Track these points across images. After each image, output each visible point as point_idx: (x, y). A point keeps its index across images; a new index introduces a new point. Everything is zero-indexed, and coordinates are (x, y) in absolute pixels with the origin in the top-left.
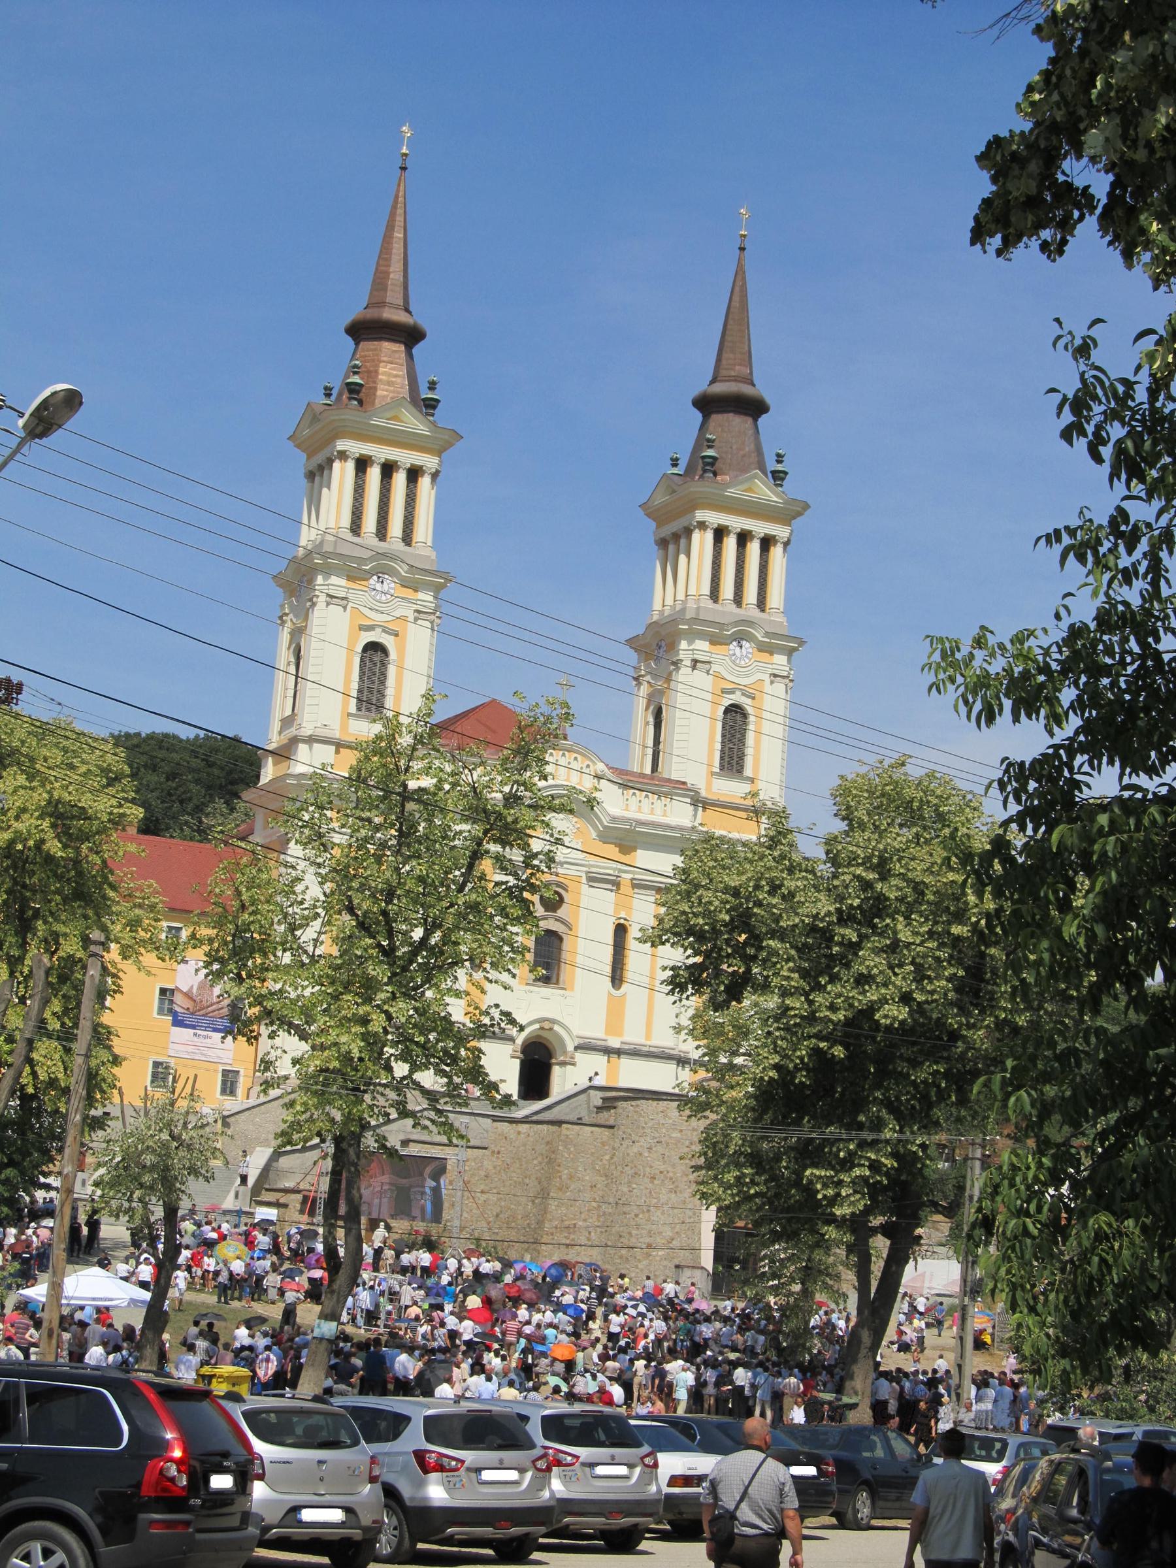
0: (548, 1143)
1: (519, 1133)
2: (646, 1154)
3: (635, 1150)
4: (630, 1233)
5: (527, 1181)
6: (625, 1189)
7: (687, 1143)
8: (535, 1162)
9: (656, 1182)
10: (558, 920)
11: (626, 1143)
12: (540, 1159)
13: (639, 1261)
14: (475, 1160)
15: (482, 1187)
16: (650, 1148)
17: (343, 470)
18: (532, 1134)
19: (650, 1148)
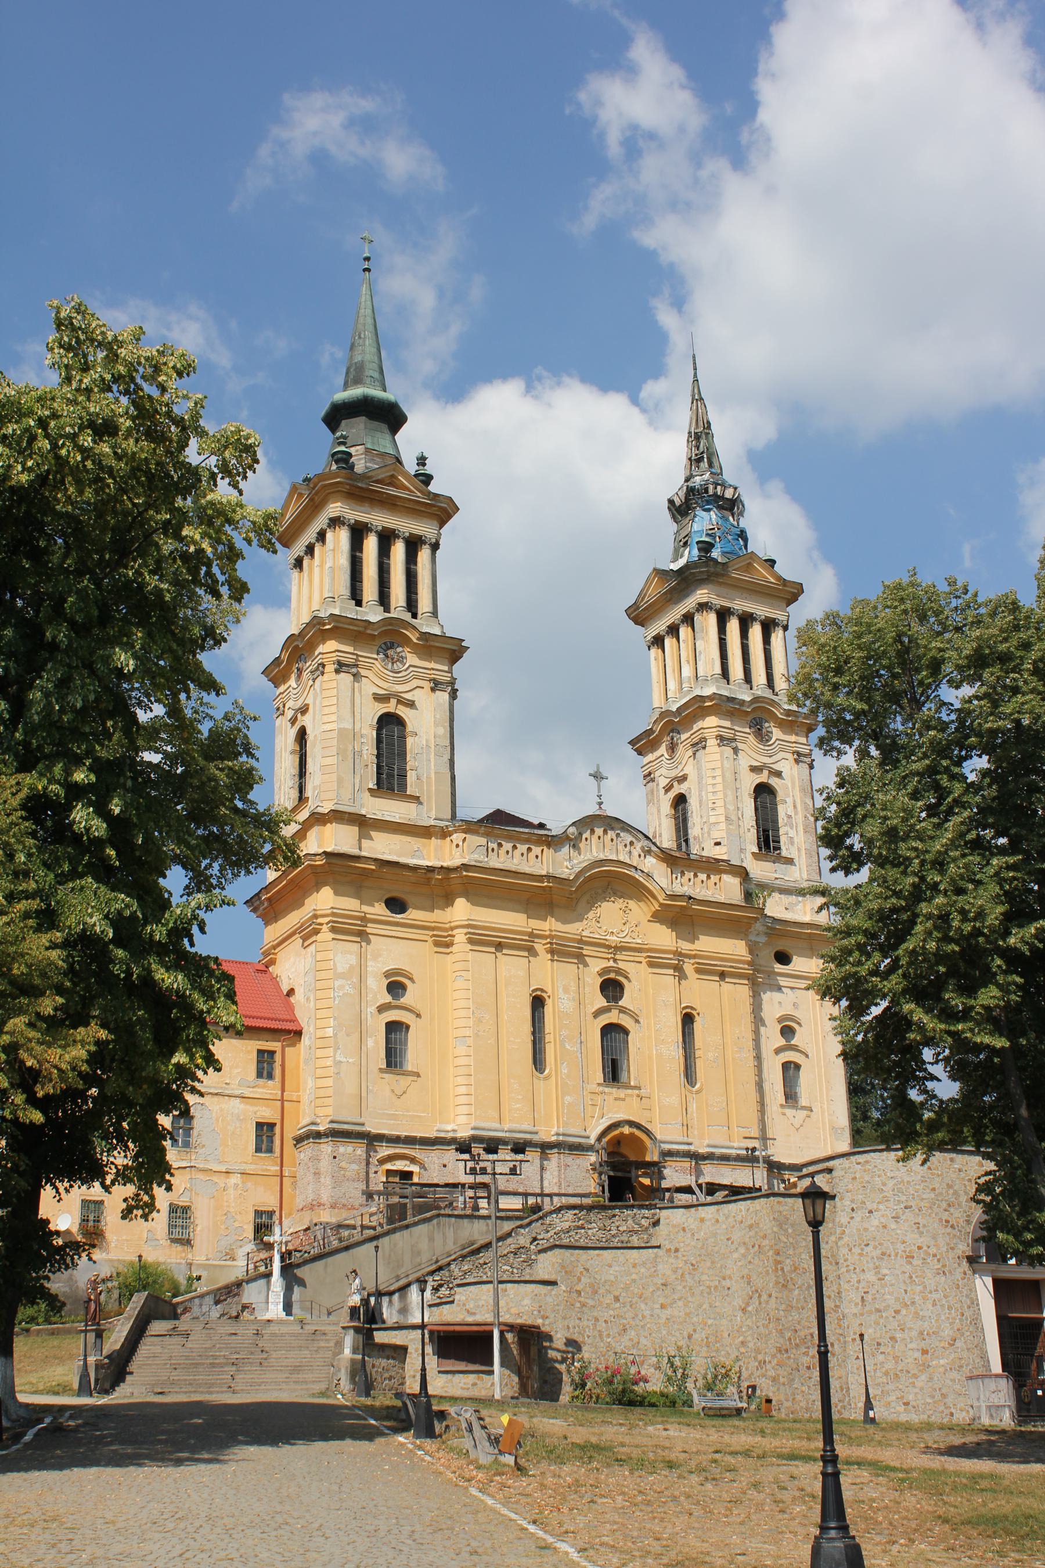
0: (751, 1227)
1: (702, 1220)
2: (893, 1226)
3: (876, 1223)
4: (893, 1338)
5: (727, 1283)
6: (871, 1276)
7: (944, 1205)
8: (736, 1255)
9: (915, 1262)
10: (623, 1010)
11: (858, 1216)
12: (742, 1250)
13: (915, 1376)
14: (644, 1264)
15: (662, 1300)
16: (896, 1218)
17: (337, 541)
18: (721, 1218)
19: (896, 1218)
